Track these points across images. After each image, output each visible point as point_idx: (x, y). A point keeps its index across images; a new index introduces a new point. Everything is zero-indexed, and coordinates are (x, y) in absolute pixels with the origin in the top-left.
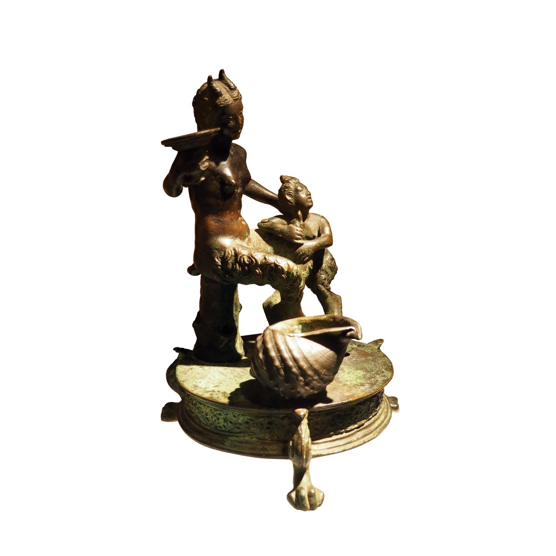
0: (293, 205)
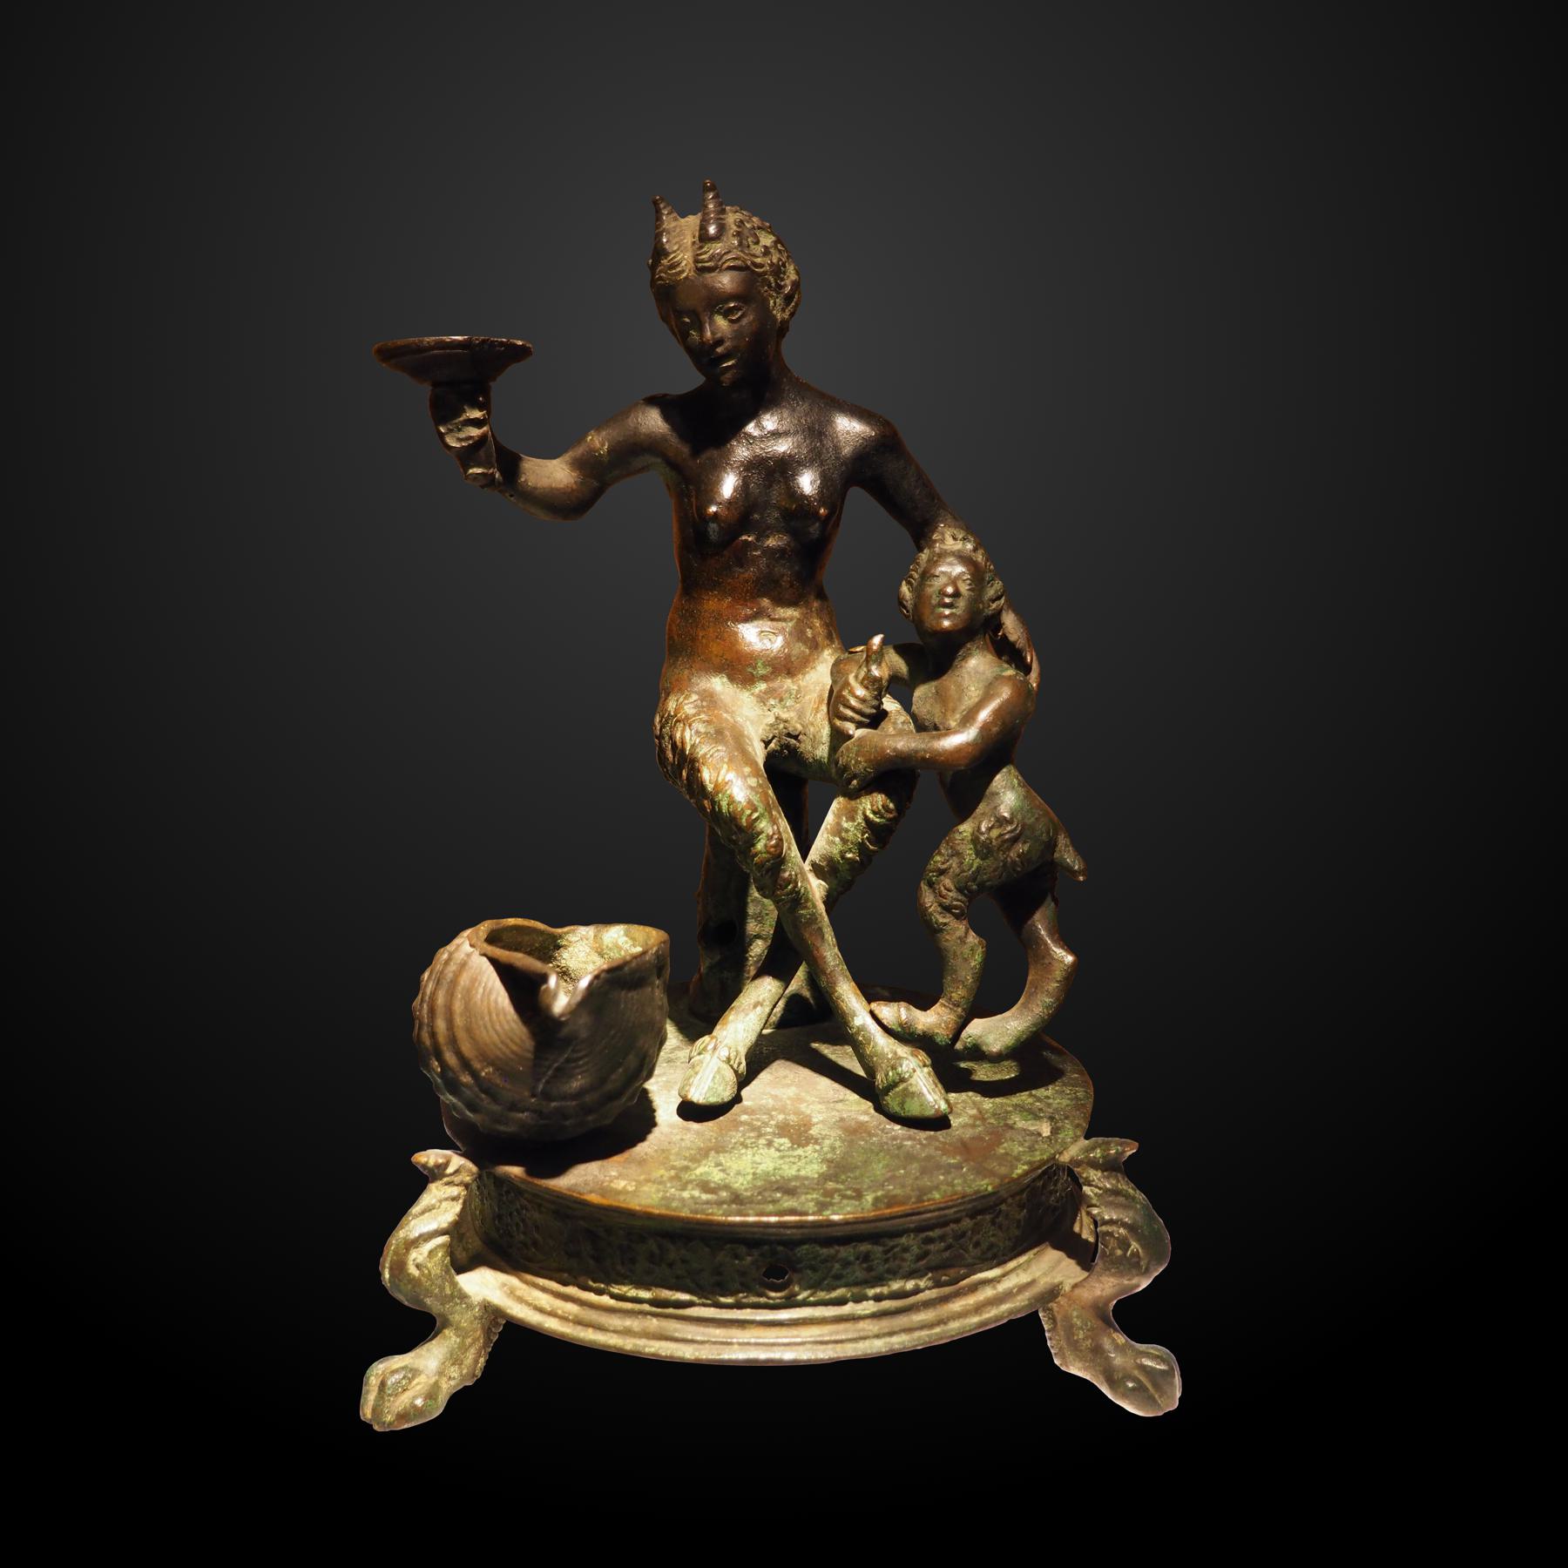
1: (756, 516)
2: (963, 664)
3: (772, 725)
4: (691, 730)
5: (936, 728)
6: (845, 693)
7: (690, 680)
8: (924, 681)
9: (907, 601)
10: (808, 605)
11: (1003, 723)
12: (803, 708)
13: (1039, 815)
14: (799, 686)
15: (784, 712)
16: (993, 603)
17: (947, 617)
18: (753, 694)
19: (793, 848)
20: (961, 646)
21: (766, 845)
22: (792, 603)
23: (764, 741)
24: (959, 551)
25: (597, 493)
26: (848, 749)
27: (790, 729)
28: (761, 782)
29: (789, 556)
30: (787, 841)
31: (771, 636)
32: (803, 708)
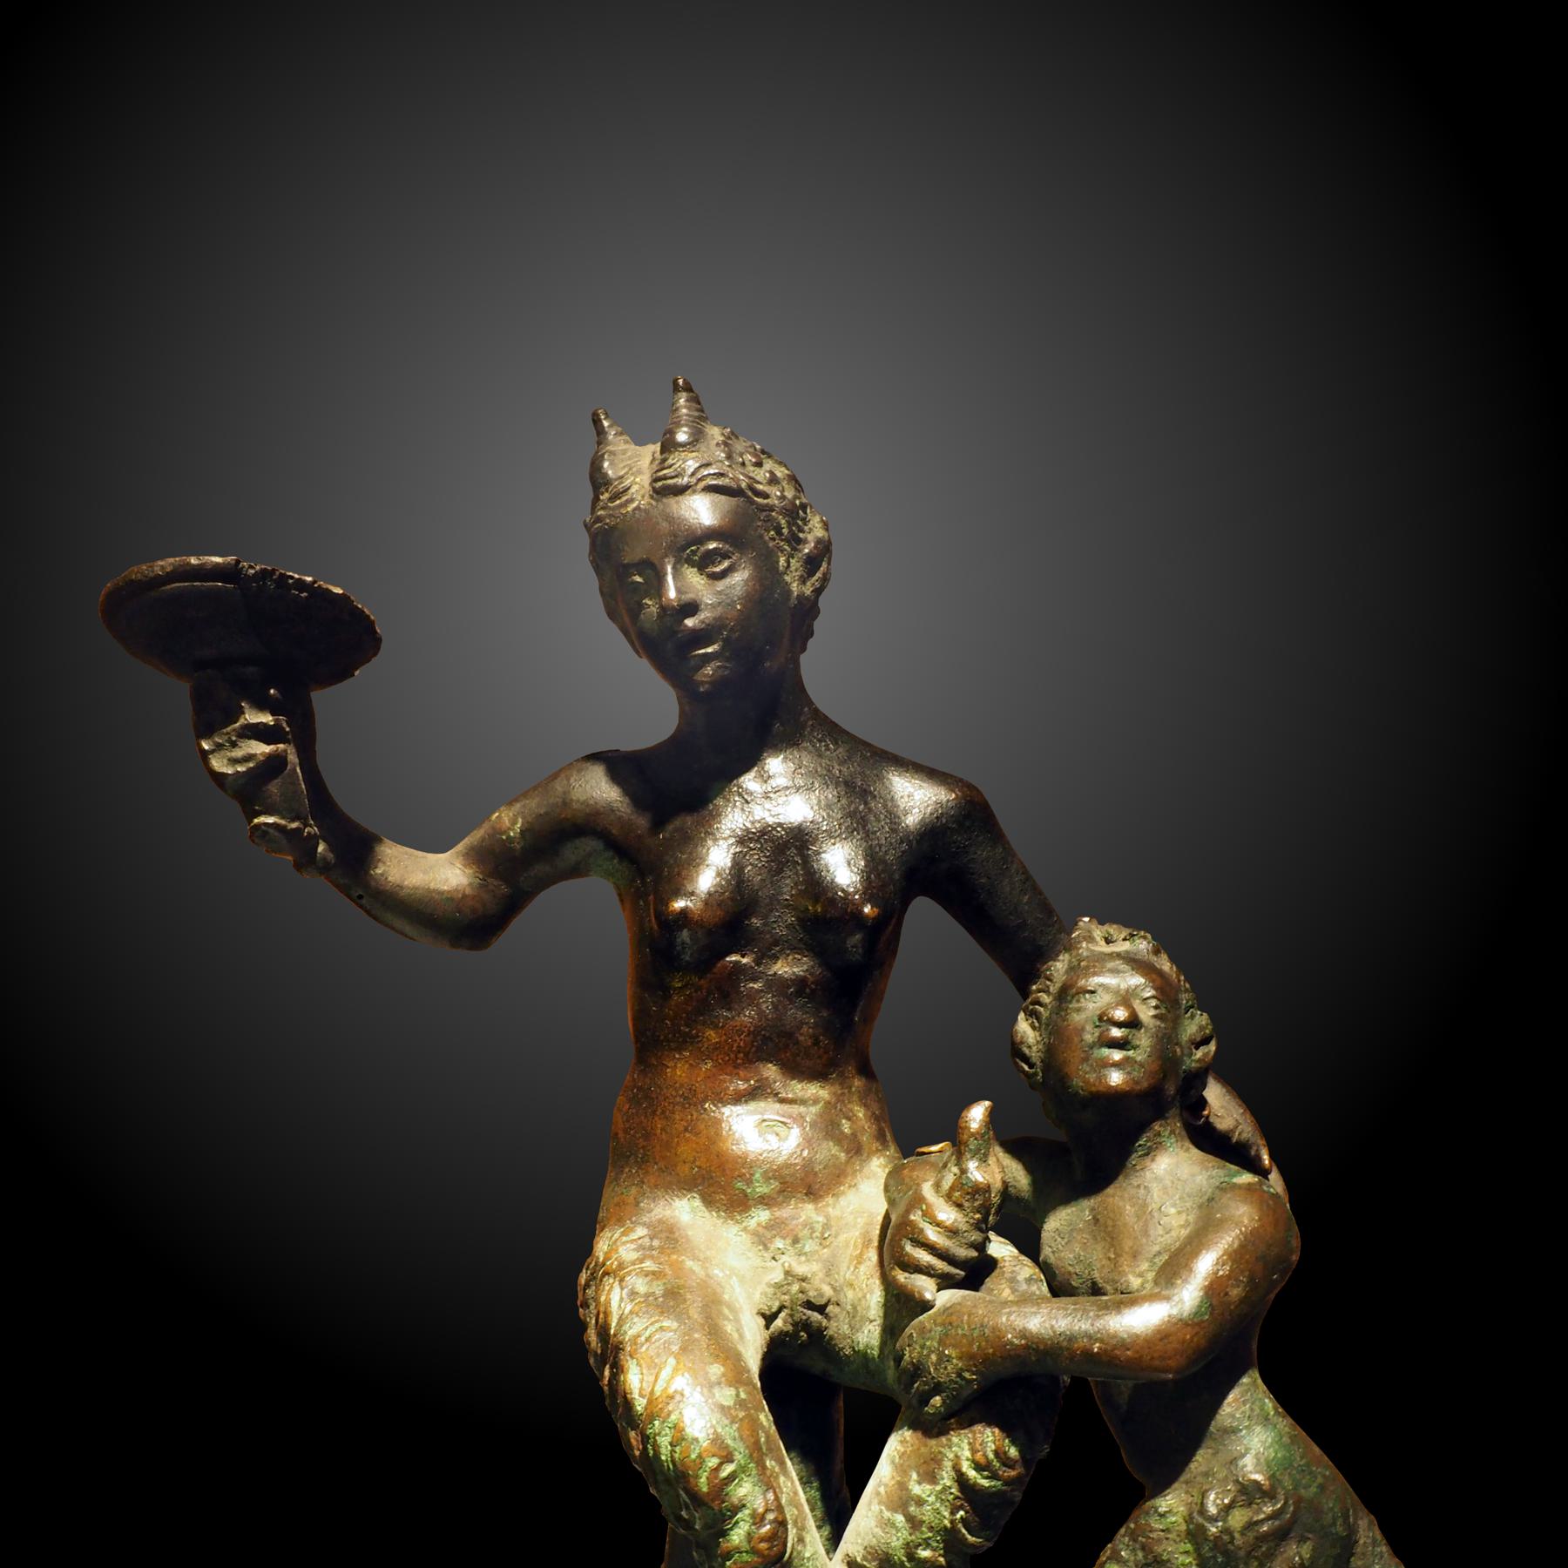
0: (1036, 1074)
1: (756, 922)
2: (1147, 1161)
3: (778, 1286)
4: (622, 1289)
5: (1096, 1290)
6: (916, 1217)
7: (637, 1204)
8: (1067, 1200)
9: (1030, 1047)
10: (843, 1081)
11: (1251, 1279)
12: (834, 1256)
13: (1324, 1476)
14: (827, 1217)
15: (800, 1263)
16: (1197, 1048)
17: (1117, 1065)
18: (745, 1230)
19: (808, 1539)
20: (1143, 1127)
21: (749, 1536)
22: (818, 1075)
23: (763, 1315)
24: (1127, 952)
25: (511, 906)
26: (922, 1330)
27: (812, 1294)
28: (743, 1396)
29: (812, 990)
30: (795, 1523)
31: (782, 1130)
32: (834, 1256)
